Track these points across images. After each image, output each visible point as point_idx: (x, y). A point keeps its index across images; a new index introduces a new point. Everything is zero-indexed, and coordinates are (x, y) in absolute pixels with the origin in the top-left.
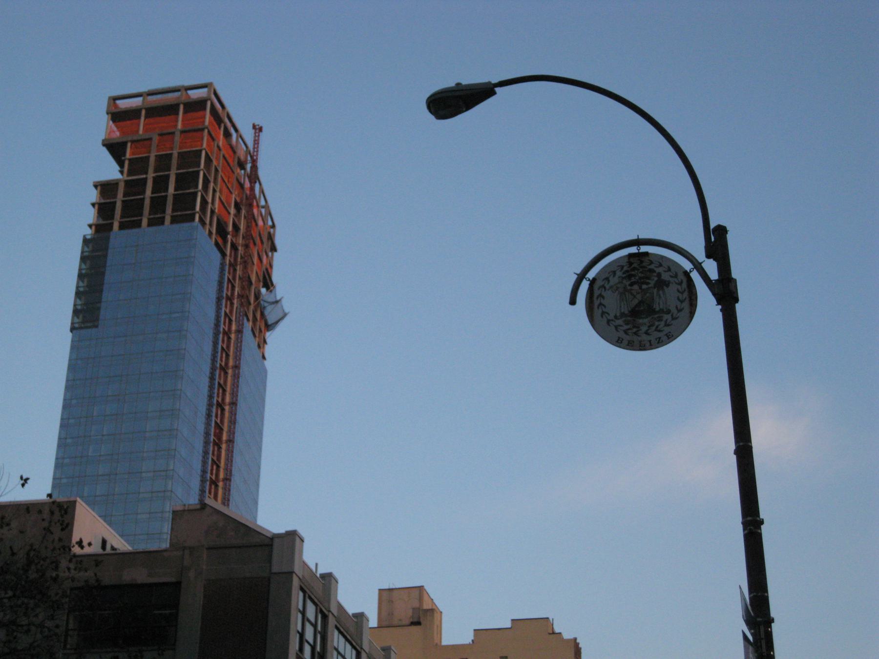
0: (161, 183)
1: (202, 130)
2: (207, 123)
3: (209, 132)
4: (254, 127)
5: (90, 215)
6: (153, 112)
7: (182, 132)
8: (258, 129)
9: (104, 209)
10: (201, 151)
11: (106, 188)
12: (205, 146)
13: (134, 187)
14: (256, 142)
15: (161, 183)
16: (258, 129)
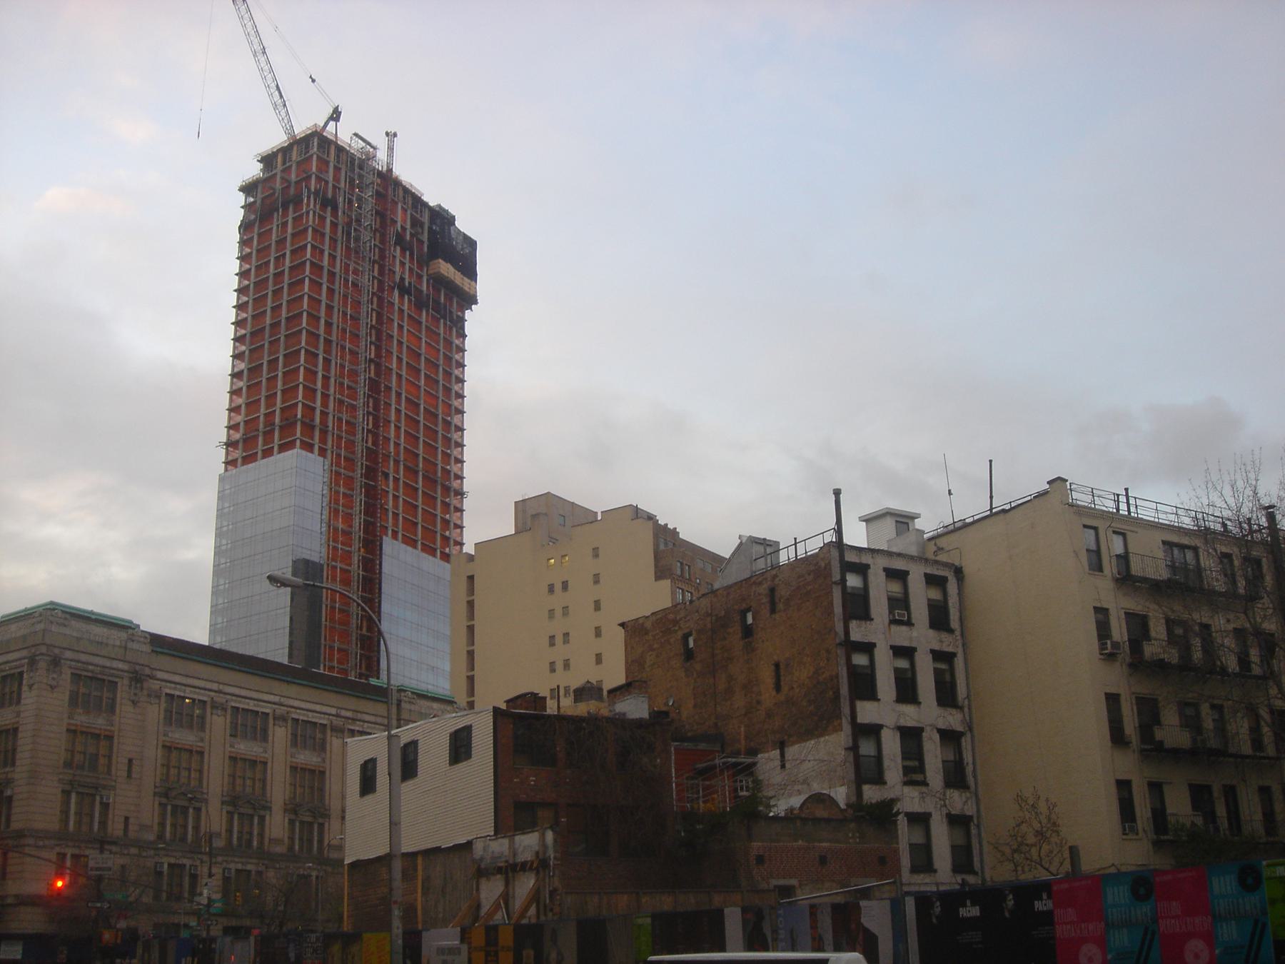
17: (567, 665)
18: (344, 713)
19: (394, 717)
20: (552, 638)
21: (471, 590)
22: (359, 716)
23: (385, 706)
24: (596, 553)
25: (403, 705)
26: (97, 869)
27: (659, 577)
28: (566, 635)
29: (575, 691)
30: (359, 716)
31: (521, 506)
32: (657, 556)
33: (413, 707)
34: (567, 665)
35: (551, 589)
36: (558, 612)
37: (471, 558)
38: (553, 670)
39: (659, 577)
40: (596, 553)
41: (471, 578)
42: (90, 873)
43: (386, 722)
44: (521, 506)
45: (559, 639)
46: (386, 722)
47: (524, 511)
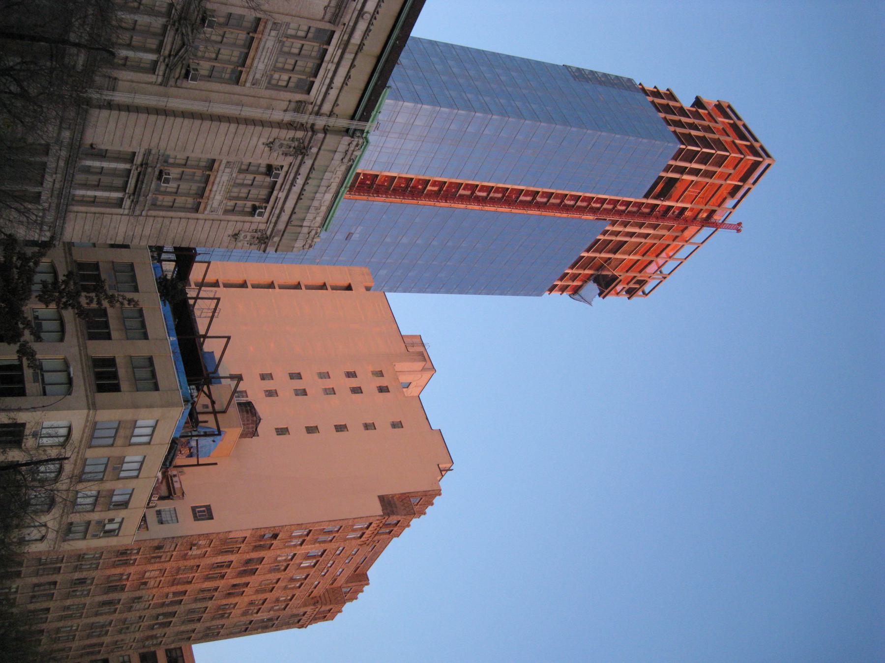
0: (694, 127)
1: (741, 153)
2: (748, 157)
3: (742, 159)
4: (740, 224)
5: (649, 86)
6: (734, 126)
7: (733, 142)
8: (738, 227)
9: (656, 94)
10: (727, 151)
11: (671, 96)
12: (733, 155)
13: (682, 111)
14: (730, 227)
15: (694, 127)
16: (738, 227)
17: (271, 393)
18: (362, 26)
19: (332, 122)
20: (299, 376)
22: (349, 57)
23: (351, 111)
24: (397, 425)
25: (347, 139)
27: (382, 499)
28: (304, 393)
30: (349, 57)
32: (405, 498)
33: (338, 156)
35: (351, 375)
38: (263, 377)
39: (382, 499)
40: (397, 425)
41: (349, 288)
43: (327, 108)
45: (298, 384)
46: (327, 108)
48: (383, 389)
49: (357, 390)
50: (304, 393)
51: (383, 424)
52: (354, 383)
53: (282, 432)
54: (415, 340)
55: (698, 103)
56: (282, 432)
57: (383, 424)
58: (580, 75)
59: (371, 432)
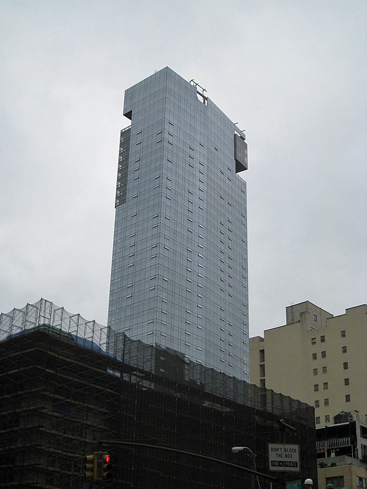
17: (327, 402)
20: (316, 386)
21: (263, 358)
24: (343, 334)
26: (281, 464)
28: (326, 384)
29: (335, 418)
31: (290, 310)
34: (327, 402)
35: (315, 356)
36: (320, 370)
37: (262, 340)
40: (343, 334)
41: (262, 352)
42: (272, 468)
44: (290, 310)
45: (321, 387)
47: (292, 313)
48: (323, 339)
49: (324, 354)
50: (326, 384)
51: (343, 342)
52: (319, 356)
53: (348, 398)
54: (290, 311)
55: (128, 115)
56: (348, 398)
57: (343, 342)
58: (121, 199)
59: (348, 349)
